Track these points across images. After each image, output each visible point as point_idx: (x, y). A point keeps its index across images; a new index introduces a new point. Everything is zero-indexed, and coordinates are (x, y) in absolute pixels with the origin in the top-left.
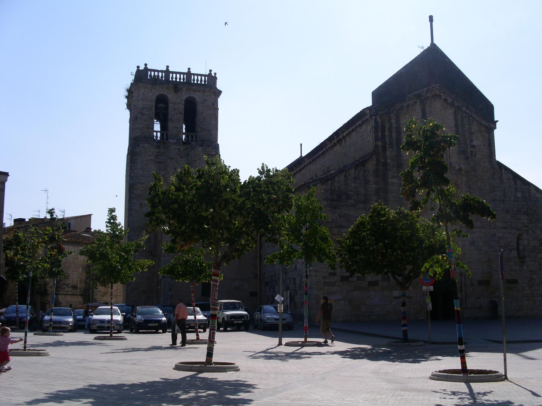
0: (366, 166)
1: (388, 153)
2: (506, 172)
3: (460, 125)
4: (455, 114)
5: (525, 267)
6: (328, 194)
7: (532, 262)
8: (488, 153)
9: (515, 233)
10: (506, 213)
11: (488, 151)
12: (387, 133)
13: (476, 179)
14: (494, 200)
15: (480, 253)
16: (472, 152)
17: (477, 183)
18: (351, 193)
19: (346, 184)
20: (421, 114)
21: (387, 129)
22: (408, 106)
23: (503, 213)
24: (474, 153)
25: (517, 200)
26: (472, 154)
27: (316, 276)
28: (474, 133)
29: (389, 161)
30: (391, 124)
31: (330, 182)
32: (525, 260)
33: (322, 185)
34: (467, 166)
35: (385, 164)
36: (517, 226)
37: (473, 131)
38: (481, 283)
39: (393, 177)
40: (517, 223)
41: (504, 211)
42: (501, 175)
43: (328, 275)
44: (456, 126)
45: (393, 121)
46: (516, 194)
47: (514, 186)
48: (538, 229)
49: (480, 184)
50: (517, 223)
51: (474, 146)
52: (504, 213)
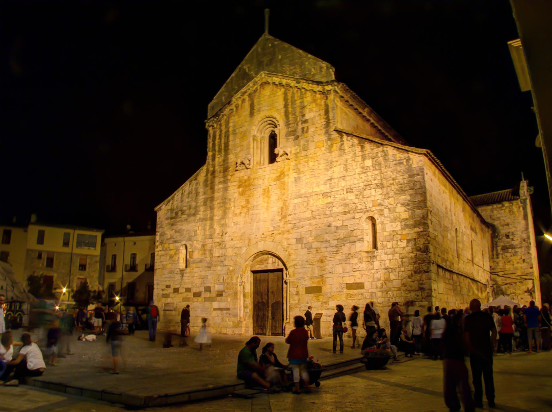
0: (198, 179)
1: (217, 160)
2: (349, 138)
3: (290, 103)
4: (285, 94)
5: (376, 264)
6: (169, 213)
7: (388, 255)
8: (325, 123)
9: (360, 217)
10: (347, 192)
11: (324, 120)
12: (217, 141)
13: (307, 159)
14: (331, 179)
15: (310, 252)
16: (303, 128)
17: (308, 164)
18: (184, 208)
19: (182, 201)
20: (249, 109)
21: (217, 137)
22: (237, 107)
23: (343, 194)
24: (305, 129)
25: (364, 171)
26: (303, 132)
27: (158, 288)
28: (307, 105)
29: (217, 168)
30: (221, 131)
31: (171, 202)
32: (376, 254)
33: (166, 206)
34: (296, 147)
35: (214, 172)
36: (364, 207)
37: (306, 104)
38: (309, 290)
39: (220, 183)
40: (364, 202)
41: (345, 190)
42: (343, 144)
43: (165, 287)
44: (286, 106)
45: (223, 128)
46: (364, 163)
47: (360, 153)
48: (399, 205)
49: (311, 164)
50: (364, 202)
51: (306, 121)
52: (345, 192)
